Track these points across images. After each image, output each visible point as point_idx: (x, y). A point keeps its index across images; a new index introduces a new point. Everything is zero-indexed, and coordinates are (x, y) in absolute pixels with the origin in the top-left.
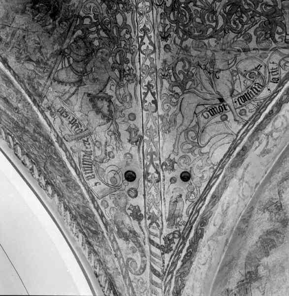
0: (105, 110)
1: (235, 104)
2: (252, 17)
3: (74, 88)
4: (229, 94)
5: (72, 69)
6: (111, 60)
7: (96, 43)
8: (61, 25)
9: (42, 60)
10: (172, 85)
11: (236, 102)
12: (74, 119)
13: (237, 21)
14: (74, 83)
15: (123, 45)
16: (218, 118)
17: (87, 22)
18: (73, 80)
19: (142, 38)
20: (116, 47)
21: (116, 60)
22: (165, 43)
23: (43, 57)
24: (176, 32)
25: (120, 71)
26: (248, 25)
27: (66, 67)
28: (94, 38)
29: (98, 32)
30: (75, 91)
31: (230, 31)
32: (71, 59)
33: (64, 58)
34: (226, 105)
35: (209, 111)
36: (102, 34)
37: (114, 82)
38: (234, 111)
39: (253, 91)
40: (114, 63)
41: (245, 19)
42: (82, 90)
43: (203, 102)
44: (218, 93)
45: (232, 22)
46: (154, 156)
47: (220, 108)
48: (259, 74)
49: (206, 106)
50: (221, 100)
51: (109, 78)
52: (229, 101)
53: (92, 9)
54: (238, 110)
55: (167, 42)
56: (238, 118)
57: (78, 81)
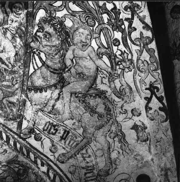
0: (101, 109)
3: (57, 92)
5: (48, 67)
7: (68, 23)
9: (5, 69)
12: (65, 131)
14: (55, 86)
15: (106, 21)
18: (53, 82)
19: (130, 21)
20: (97, 24)
21: (102, 44)
23: (6, 64)
25: (109, 58)
27: (39, 68)
28: (65, 16)
30: (59, 94)
32: (43, 55)
33: (33, 56)
37: (105, 72)
40: (99, 47)
46: (169, 173)
51: (97, 69)
57: (59, 82)
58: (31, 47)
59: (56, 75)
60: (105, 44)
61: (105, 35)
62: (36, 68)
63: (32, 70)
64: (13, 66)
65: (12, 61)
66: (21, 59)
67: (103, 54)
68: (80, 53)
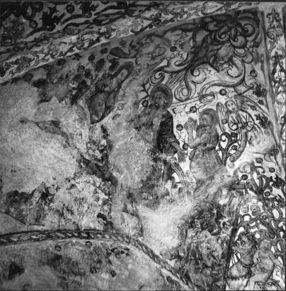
3: (246, 280)
5: (242, 263)
6: (273, 249)
7: (257, 236)
8: (225, 226)
14: (245, 276)
15: (282, 236)
17: (247, 218)
18: (244, 273)
20: (276, 237)
21: (278, 249)
23: (216, 259)
28: (255, 232)
29: (257, 226)
30: (247, 282)
32: (239, 255)
33: (233, 255)
36: (262, 227)
37: (279, 268)
40: (276, 251)
42: (252, 280)
51: (274, 265)
53: (249, 208)
57: (248, 273)
58: (232, 249)
59: (246, 269)
60: (280, 250)
61: (280, 244)
62: (234, 263)
63: (231, 265)
64: (220, 261)
65: (220, 258)
66: (225, 257)
67: (278, 256)
68: (263, 254)
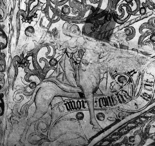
1: (95, 104)
2: (144, 8)
4: (91, 90)
10: (28, 75)
11: (96, 102)
13: (125, 8)
16: (73, 114)
22: (27, 25)
24: (46, 11)
26: (136, 17)
31: (112, 19)
34: (86, 102)
35: (65, 104)
38: (92, 111)
39: (118, 97)
41: (134, 8)
43: (61, 93)
44: (81, 87)
45: (118, 7)
47: (79, 103)
48: (130, 80)
49: (64, 98)
50: (82, 95)
52: (90, 98)
54: (96, 112)
55: (30, 23)
56: (94, 121)
